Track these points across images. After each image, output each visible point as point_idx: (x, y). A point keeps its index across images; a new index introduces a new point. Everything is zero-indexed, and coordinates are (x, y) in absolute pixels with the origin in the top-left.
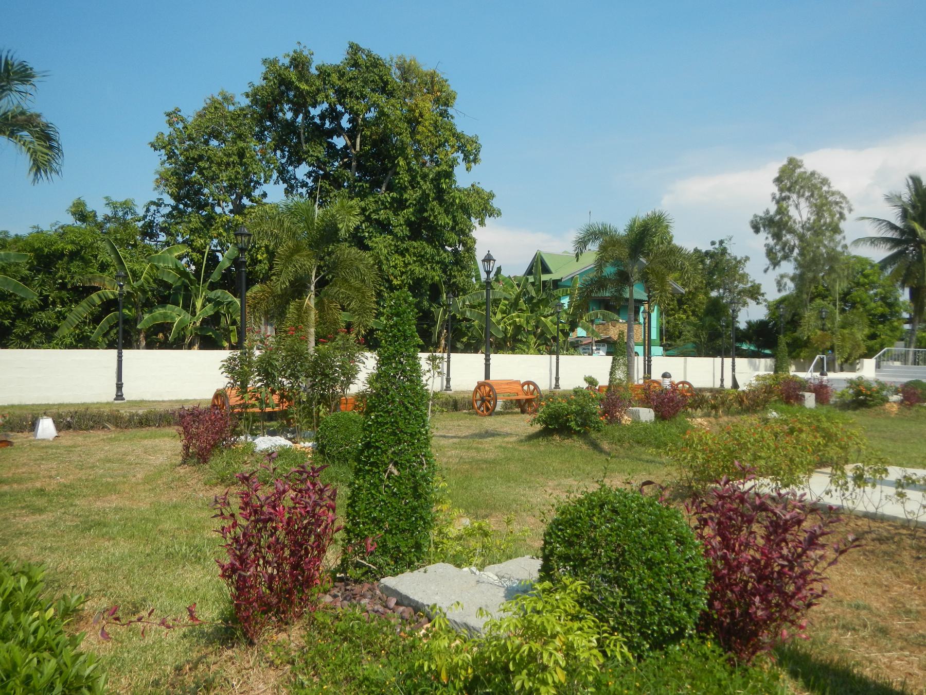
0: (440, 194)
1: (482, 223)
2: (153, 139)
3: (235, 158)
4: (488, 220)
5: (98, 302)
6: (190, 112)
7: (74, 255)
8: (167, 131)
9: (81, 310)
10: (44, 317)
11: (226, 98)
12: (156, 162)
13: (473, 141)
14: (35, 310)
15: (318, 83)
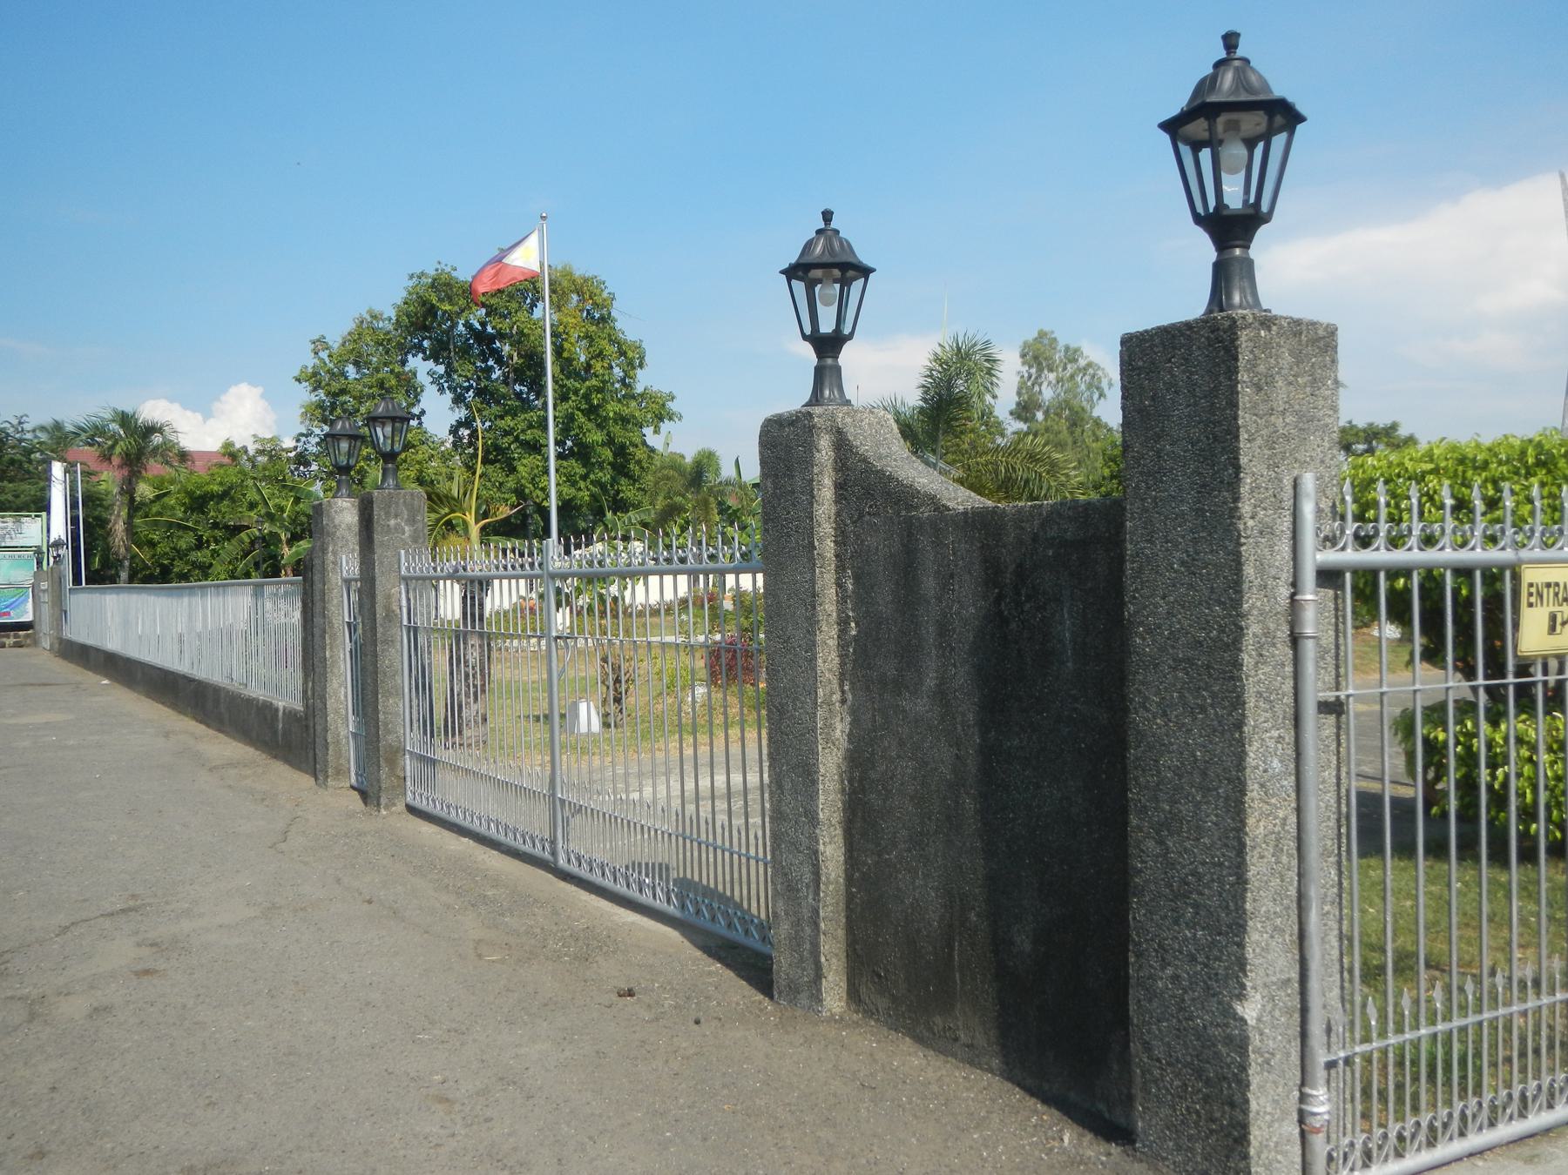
0: (592, 411)
1: (657, 431)
2: (296, 373)
3: (375, 390)
4: (666, 426)
5: (247, 540)
6: (335, 340)
7: (225, 495)
8: (310, 362)
9: (231, 548)
10: (200, 556)
11: (374, 317)
12: (304, 395)
13: (638, 347)
14: (190, 549)
15: (462, 302)
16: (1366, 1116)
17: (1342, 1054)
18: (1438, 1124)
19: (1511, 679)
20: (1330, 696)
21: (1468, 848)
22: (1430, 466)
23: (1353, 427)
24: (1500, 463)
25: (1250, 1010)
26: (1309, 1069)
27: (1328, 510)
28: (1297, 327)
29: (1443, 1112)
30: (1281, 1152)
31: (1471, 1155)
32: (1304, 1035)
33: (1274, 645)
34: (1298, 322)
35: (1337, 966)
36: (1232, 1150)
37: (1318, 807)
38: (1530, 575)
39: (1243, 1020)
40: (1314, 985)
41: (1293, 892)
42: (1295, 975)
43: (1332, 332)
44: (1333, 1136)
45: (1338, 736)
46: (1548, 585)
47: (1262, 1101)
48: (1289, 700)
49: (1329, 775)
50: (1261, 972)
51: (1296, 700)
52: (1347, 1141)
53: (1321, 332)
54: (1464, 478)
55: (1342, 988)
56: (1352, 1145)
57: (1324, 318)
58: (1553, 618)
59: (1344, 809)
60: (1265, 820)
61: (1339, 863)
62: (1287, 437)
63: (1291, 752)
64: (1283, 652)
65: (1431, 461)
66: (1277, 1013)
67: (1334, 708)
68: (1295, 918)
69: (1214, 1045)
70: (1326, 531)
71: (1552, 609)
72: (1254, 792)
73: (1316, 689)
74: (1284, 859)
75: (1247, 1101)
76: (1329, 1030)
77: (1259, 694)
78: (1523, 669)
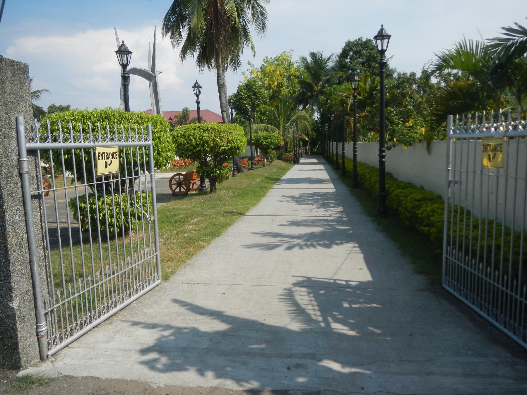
16: (60, 327)
17: (50, 309)
18: (83, 322)
19: (95, 183)
20: (36, 193)
21: (95, 239)
22: (73, 118)
23: (54, 106)
24: (94, 118)
25: (15, 305)
26: (38, 317)
27: (30, 129)
28: (12, 63)
29: (84, 318)
30: (31, 348)
31: (94, 328)
32: (36, 307)
33: (13, 177)
34: (13, 61)
35: (46, 282)
36: (13, 353)
37: (34, 231)
38: (99, 150)
39: (13, 308)
40: (38, 289)
41: (28, 260)
42: (31, 288)
43: (26, 66)
44: (49, 336)
45: (40, 206)
46: (104, 153)
47: (22, 333)
48: (20, 195)
49: (38, 220)
50: (18, 290)
51: (23, 195)
52: (54, 336)
53: (22, 66)
54: (84, 122)
55: (48, 288)
56: (56, 337)
57: (23, 61)
58: (106, 163)
59: (44, 230)
60: (14, 238)
61: (44, 248)
62: (12, 103)
63: (22, 213)
64: (17, 179)
65: (73, 116)
66: (25, 302)
67: (37, 197)
68: (29, 269)
69: (3, 320)
70: (30, 136)
71: (106, 160)
72: (9, 229)
73: (30, 191)
74: (24, 250)
75: (17, 335)
76: (45, 303)
77: (8, 194)
78: (99, 179)
